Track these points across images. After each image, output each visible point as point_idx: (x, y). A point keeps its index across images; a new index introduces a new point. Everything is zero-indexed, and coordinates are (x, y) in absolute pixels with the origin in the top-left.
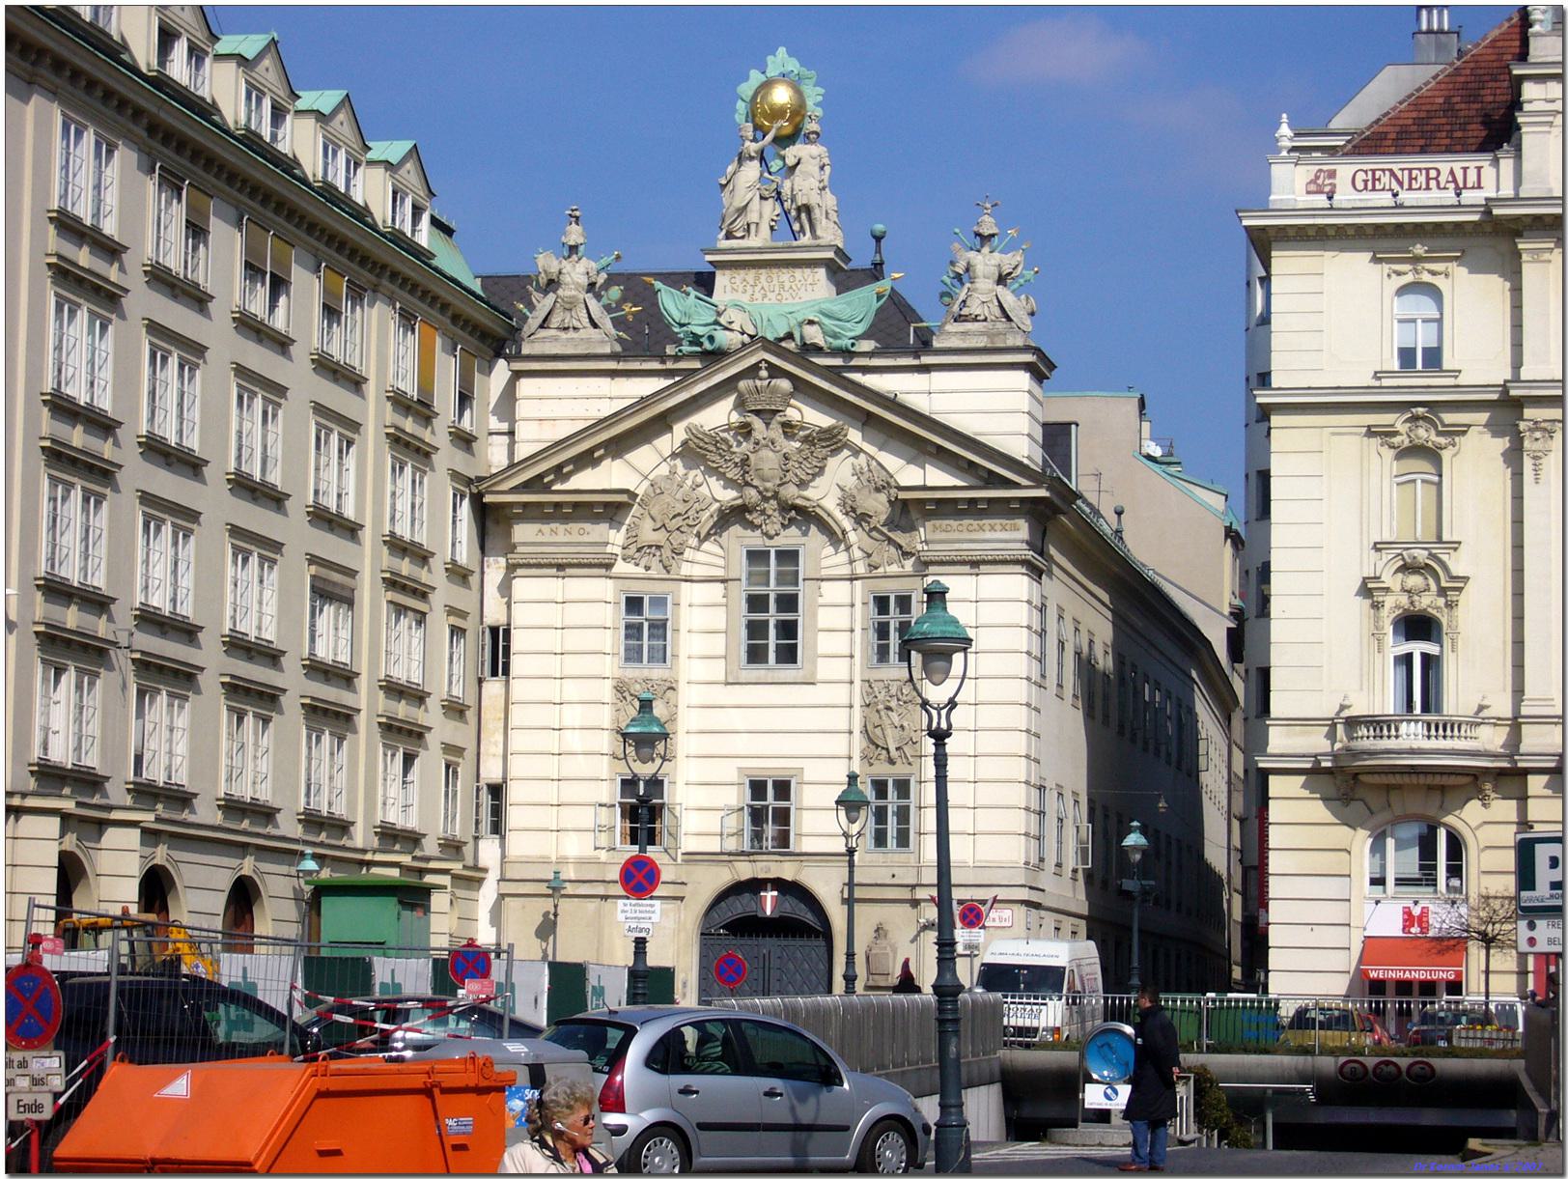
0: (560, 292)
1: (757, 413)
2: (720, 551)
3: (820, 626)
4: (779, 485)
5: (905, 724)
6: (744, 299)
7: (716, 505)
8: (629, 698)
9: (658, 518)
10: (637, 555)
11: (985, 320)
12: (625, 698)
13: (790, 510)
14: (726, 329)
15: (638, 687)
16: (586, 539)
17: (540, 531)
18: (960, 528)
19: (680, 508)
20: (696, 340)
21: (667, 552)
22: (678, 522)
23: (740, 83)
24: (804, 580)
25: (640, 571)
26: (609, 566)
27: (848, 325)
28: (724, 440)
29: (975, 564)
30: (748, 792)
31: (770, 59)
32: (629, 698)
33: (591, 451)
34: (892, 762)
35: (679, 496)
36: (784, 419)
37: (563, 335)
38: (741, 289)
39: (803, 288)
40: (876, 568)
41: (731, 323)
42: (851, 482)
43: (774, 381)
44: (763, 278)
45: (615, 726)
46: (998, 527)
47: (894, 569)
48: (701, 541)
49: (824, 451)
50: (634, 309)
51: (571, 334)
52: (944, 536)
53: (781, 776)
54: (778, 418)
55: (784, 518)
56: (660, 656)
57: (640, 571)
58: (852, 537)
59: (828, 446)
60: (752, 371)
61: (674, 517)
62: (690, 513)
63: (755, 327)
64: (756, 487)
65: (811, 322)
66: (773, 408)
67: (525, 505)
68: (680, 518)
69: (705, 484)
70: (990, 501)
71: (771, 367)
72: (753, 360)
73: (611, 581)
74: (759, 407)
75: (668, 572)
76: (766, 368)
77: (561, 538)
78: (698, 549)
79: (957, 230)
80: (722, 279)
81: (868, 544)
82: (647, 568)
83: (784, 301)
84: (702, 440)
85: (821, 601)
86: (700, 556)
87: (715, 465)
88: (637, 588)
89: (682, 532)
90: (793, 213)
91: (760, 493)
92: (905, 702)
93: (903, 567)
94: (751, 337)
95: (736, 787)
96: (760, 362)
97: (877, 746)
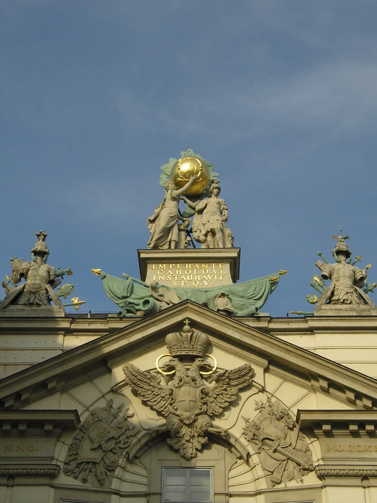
4: (198, 415)
7: (144, 432)
10: (76, 470)
11: (350, 303)
14: (157, 300)
16: (36, 454)
22: (112, 445)
23: (160, 176)
24: (215, 494)
25: (77, 483)
26: (53, 476)
27: (251, 301)
29: (365, 477)
33: (44, 384)
37: (28, 308)
41: (161, 296)
47: (292, 484)
51: (35, 308)
52: (337, 455)
54: (198, 362)
57: (77, 483)
58: (255, 459)
61: (110, 439)
62: (121, 438)
65: (223, 295)
66: (194, 353)
68: (114, 442)
71: (194, 324)
72: (179, 318)
73: (53, 489)
74: (183, 353)
75: (102, 485)
76: (189, 324)
78: (124, 468)
81: (271, 464)
82: (85, 481)
84: (136, 377)
86: (128, 476)
89: (115, 453)
93: (302, 481)
96: (185, 320)
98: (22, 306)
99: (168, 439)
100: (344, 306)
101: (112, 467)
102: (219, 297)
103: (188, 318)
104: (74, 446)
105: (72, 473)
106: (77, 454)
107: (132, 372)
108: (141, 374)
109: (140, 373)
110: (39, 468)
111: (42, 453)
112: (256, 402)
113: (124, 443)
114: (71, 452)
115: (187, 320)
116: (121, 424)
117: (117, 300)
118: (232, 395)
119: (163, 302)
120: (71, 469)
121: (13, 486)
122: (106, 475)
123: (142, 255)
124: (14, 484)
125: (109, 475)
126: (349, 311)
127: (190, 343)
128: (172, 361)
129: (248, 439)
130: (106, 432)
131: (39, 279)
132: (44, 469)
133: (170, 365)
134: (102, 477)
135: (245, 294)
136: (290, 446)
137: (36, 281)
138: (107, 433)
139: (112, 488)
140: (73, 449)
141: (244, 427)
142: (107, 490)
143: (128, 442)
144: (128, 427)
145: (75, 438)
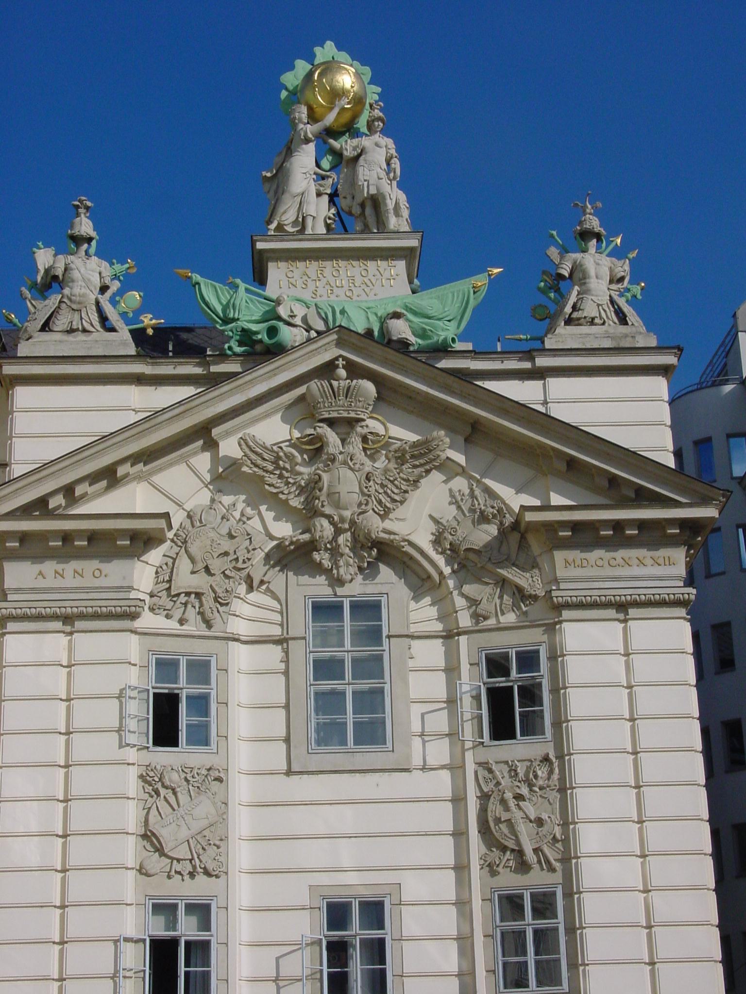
0: (67, 291)
1: (331, 423)
2: (275, 604)
3: (413, 695)
5: (545, 816)
6: (307, 296)
8: (163, 791)
9: (198, 558)
11: (603, 324)
12: (158, 793)
13: (371, 548)
15: (175, 776)
17: (40, 573)
18: (599, 563)
19: (227, 545)
20: (246, 338)
21: (208, 601)
24: (389, 637)
25: (172, 625)
26: (133, 616)
27: (440, 323)
28: (290, 457)
30: (323, 917)
31: (318, 50)
32: (163, 791)
34: (523, 866)
35: (224, 531)
36: (365, 431)
38: (299, 284)
39: (379, 282)
40: (486, 618)
42: (449, 513)
43: (355, 381)
44: (328, 272)
45: (143, 832)
46: (648, 561)
47: (510, 618)
48: (250, 588)
49: (417, 471)
50: (154, 321)
53: (369, 894)
54: (359, 429)
55: (361, 558)
56: (201, 737)
57: (172, 625)
59: (421, 465)
60: (327, 370)
63: (326, 321)
64: (329, 517)
65: (396, 315)
66: (353, 415)
67: (24, 537)
69: (257, 517)
70: (642, 525)
72: (327, 357)
73: (137, 637)
74: (334, 415)
76: (344, 367)
77: (70, 581)
79: (554, 233)
80: (276, 272)
83: (355, 298)
85: (411, 663)
87: (275, 491)
88: (170, 646)
90: (356, 210)
91: (332, 523)
92: (541, 788)
94: (319, 333)
95: (307, 912)
96: (337, 359)
97: (504, 849)
98: (60, 334)
99: (315, 553)
100: (594, 329)
101: (226, 599)
102: (391, 318)
103: (340, 356)
104: (164, 567)
105: (164, 610)
106: (170, 581)
107: (254, 448)
108: (268, 450)
109: (266, 448)
110: (113, 605)
111: (113, 580)
112: (450, 490)
113: (244, 560)
114: (161, 579)
115: (341, 359)
116: (237, 531)
117: (221, 326)
118: (414, 481)
119: (298, 328)
120: (161, 604)
121: (71, 633)
122: (218, 612)
123: (260, 245)
124: (73, 629)
125: (223, 612)
126: (601, 337)
127: (346, 397)
128: (317, 428)
129: (440, 550)
130: (214, 545)
131: (84, 287)
132: (121, 607)
133: (313, 434)
134: (211, 615)
135: (430, 312)
136: (506, 560)
137: (80, 289)
138: (216, 546)
139: (228, 631)
140: (163, 572)
141: (434, 531)
142: (222, 635)
143: (249, 559)
144: (248, 534)
145: (164, 556)
